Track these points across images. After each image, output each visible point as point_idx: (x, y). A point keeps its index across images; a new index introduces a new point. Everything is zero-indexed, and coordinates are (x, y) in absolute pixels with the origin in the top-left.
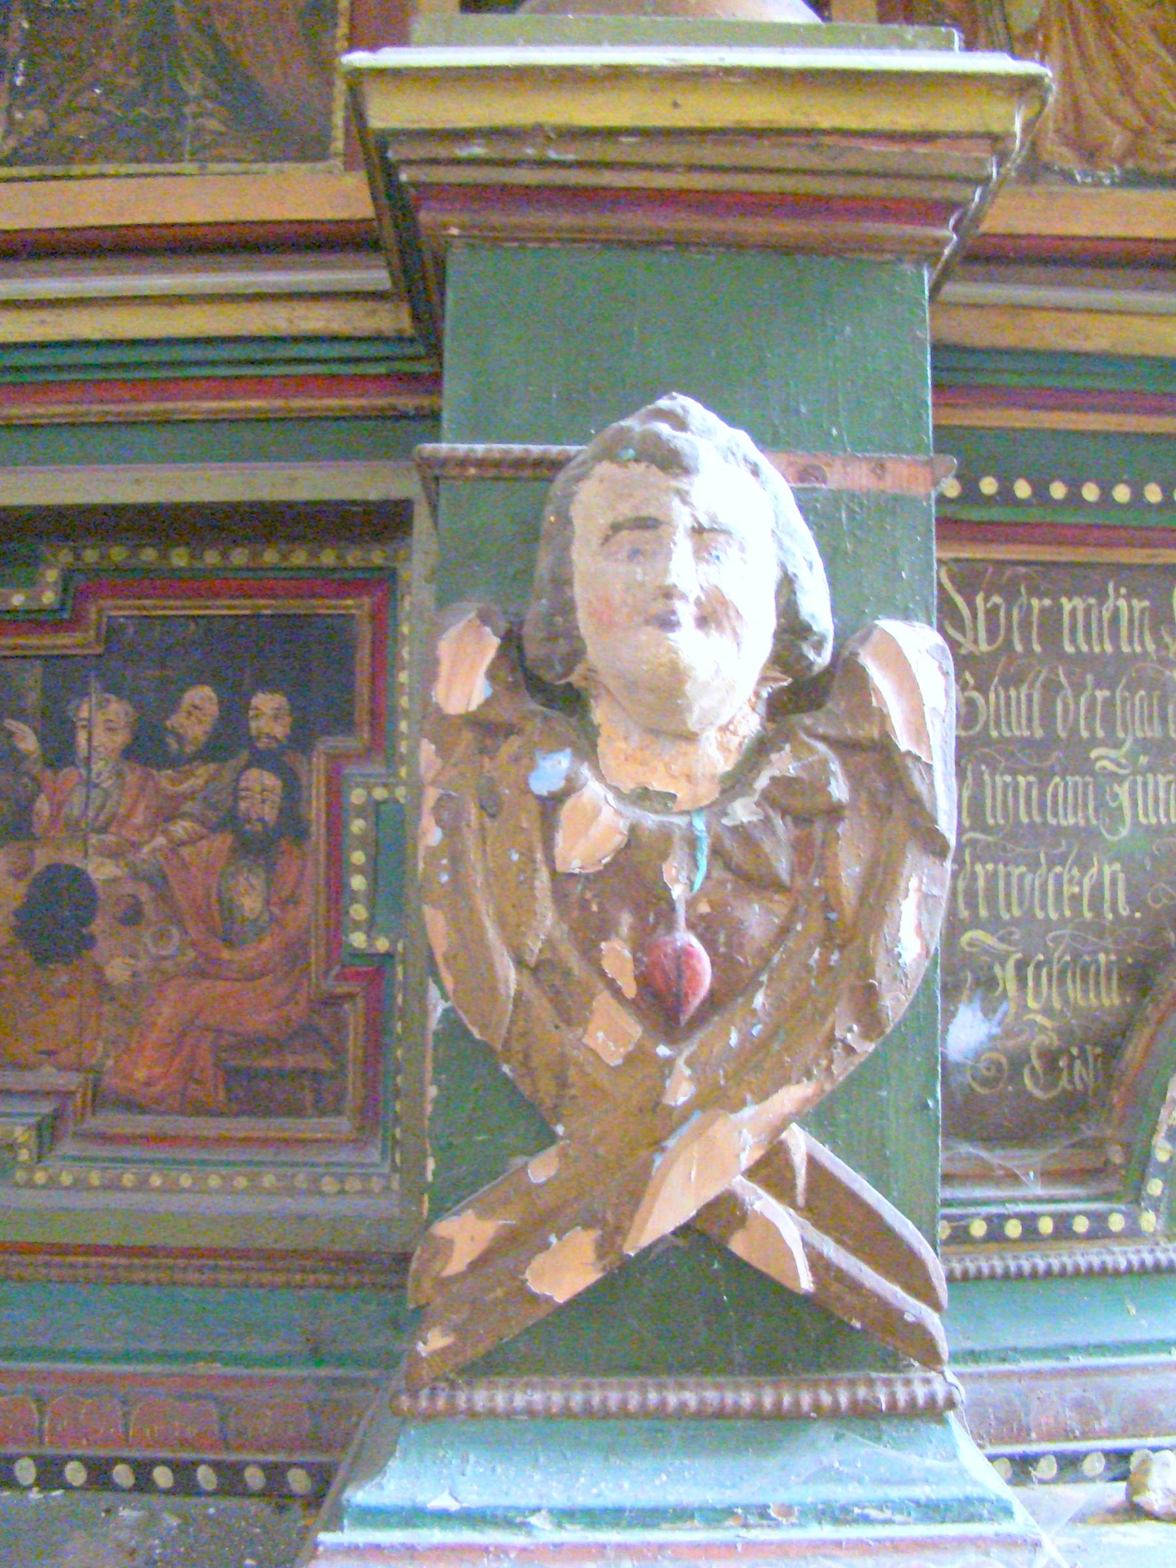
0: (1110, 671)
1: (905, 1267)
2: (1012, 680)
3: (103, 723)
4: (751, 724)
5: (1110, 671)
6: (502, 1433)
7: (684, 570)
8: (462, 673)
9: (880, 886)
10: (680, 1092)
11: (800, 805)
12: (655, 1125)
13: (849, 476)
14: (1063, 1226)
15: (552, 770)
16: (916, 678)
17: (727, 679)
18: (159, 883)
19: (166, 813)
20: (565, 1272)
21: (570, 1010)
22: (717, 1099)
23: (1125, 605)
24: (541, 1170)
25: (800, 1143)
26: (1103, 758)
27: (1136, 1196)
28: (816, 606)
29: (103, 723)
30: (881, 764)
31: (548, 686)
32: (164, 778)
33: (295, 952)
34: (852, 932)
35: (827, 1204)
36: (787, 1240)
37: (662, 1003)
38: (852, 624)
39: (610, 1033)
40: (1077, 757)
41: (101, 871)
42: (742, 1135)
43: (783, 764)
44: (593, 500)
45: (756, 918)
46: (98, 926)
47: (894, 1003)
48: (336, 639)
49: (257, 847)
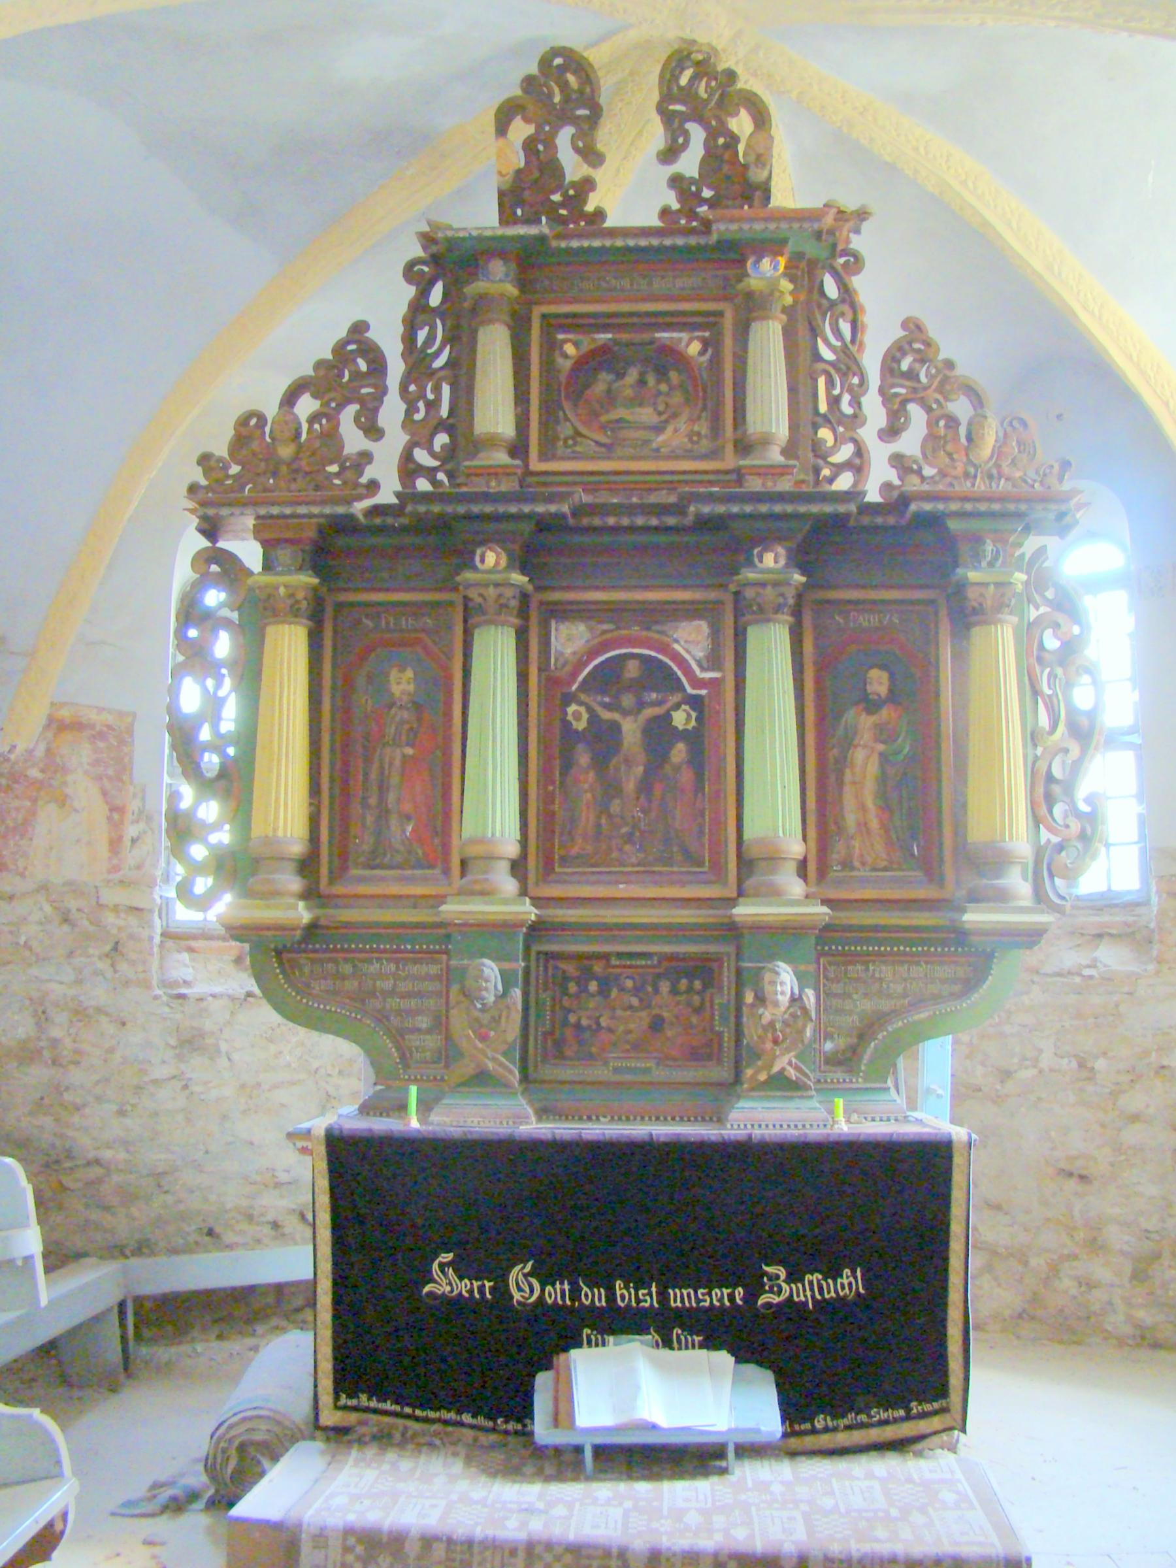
0: (858, 980)
1: (806, 1075)
2: (838, 982)
3: (665, 987)
4: (787, 1004)
5: (858, 980)
6: (753, 1098)
7: (779, 988)
8: (749, 998)
9: (804, 1026)
10: (778, 1053)
11: (794, 1016)
12: (775, 1058)
13: (802, 968)
14: (844, 1081)
15: (761, 1011)
16: (810, 996)
17: (784, 1000)
18: (677, 1017)
19: (678, 1003)
20: (763, 1077)
21: (764, 1043)
22: (782, 1054)
23: (859, 967)
24: (760, 1063)
25: (794, 1060)
26: (855, 996)
27: (858, 1076)
28: (796, 991)
29: (665, 987)
30: (804, 1010)
31: (761, 999)
32: (678, 998)
33: (704, 1030)
34: (801, 1032)
35: (797, 1068)
36: (792, 1073)
37: (776, 1042)
38: (801, 990)
39: (769, 1045)
40: (849, 996)
41: (666, 1015)
42: (786, 1059)
43: (791, 1010)
44: (767, 977)
45: (788, 1030)
46: (665, 1025)
47: (806, 1041)
48: (711, 970)
49: (698, 1010)
